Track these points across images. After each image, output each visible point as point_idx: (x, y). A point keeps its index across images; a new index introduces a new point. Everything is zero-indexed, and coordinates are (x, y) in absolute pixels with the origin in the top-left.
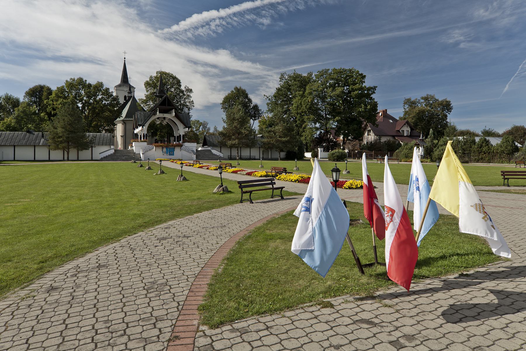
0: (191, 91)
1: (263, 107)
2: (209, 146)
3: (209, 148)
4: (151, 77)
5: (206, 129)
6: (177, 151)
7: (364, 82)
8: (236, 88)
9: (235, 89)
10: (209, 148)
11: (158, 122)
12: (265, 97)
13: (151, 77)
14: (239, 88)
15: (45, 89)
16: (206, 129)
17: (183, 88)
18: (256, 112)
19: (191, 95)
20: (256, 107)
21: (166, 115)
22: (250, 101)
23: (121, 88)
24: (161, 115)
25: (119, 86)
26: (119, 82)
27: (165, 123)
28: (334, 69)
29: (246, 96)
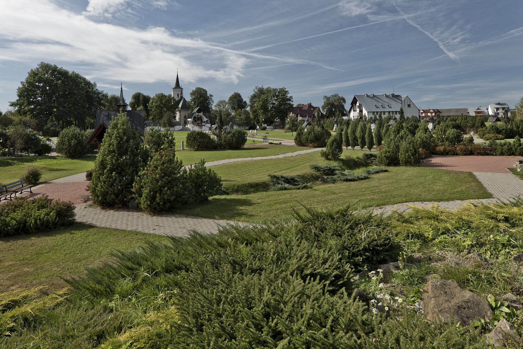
0: (212, 96)
1: (248, 102)
4: (193, 91)
6: (203, 127)
11: (197, 116)
13: (193, 91)
15: (141, 95)
17: (208, 95)
19: (212, 98)
20: (245, 102)
21: (199, 114)
22: (242, 99)
23: (176, 90)
24: (198, 114)
25: (175, 88)
26: (174, 85)
27: (199, 116)
28: (273, 89)
29: (240, 97)
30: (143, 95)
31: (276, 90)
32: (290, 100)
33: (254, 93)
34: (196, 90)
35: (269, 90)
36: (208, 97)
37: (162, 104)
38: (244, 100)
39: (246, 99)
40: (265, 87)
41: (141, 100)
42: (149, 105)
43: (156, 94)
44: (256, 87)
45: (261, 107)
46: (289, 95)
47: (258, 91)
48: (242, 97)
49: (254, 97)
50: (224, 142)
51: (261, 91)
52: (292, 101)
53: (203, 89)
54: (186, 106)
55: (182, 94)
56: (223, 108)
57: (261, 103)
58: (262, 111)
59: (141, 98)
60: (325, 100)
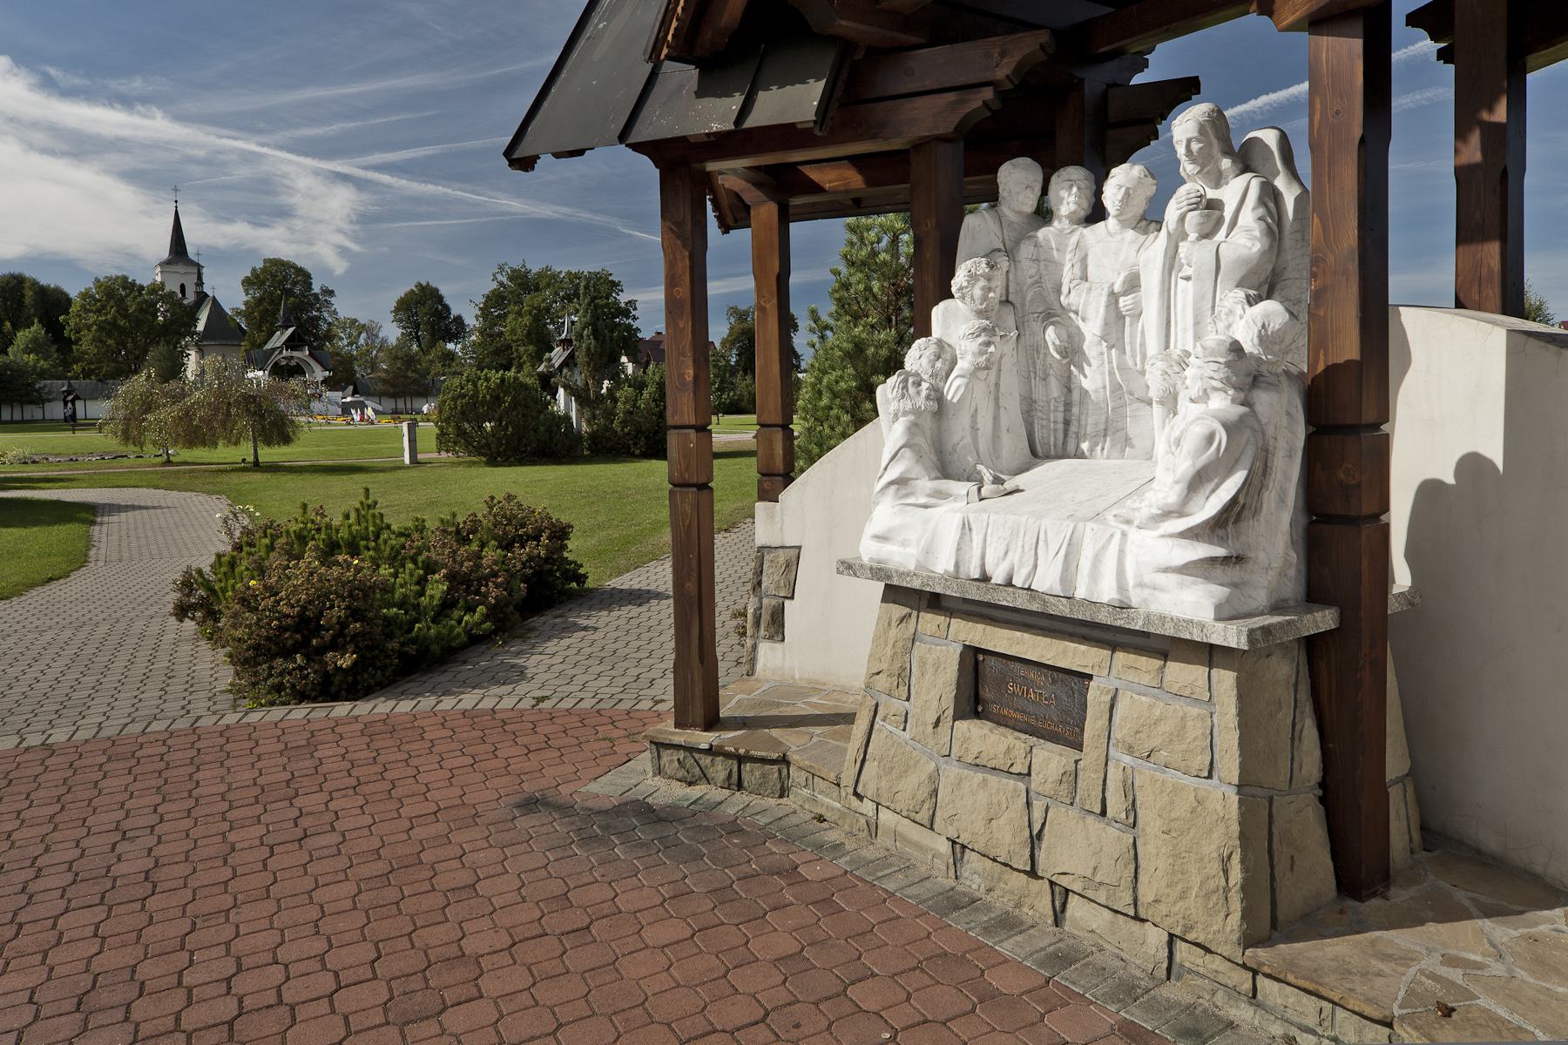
0: (331, 293)
1: (471, 319)
2: (361, 395)
3: (362, 399)
4: (254, 270)
5: (378, 341)
7: (622, 291)
8: (419, 285)
9: (416, 286)
10: (362, 399)
12: (473, 305)
14: (424, 284)
15: (27, 285)
16: (378, 341)
17: (316, 289)
18: (456, 329)
19: (333, 300)
20: (459, 320)
21: (295, 354)
22: (447, 308)
23: (172, 268)
26: (164, 253)
27: (293, 363)
28: (569, 273)
29: (440, 299)
30: (35, 283)
31: (577, 276)
32: (625, 313)
33: (494, 285)
34: (264, 270)
35: (548, 279)
36: (316, 295)
37: (125, 316)
38: (454, 312)
39: (468, 307)
40: (535, 268)
41: (28, 301)
42: (70, 321)
43: (97, 280)
44: (501, 269)
45: (529, 334)
46: (623, 298)
47: (511, 279)
48: (447, 301)
49: (496, 300)
50: (624, 423)
51: (523, 283)
52: (635, 318)
53: (294, 266)
54: (223, 330)
55: (200, 283)
56: (350, 344)
57: (527, 320)
58: (531, 348)
59: (29, 294)
60: (732, 320)
